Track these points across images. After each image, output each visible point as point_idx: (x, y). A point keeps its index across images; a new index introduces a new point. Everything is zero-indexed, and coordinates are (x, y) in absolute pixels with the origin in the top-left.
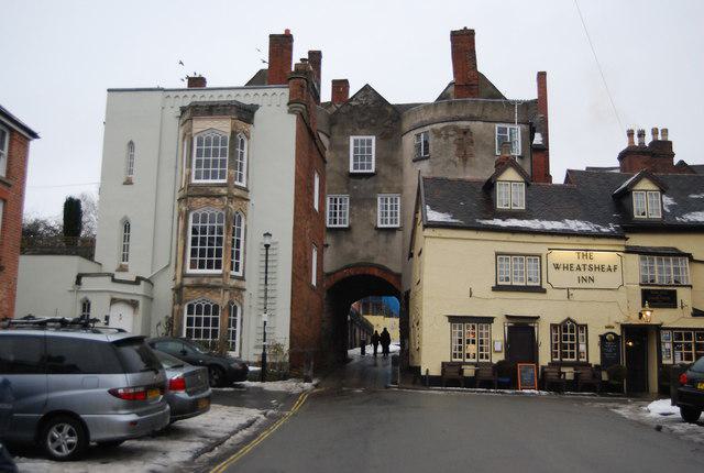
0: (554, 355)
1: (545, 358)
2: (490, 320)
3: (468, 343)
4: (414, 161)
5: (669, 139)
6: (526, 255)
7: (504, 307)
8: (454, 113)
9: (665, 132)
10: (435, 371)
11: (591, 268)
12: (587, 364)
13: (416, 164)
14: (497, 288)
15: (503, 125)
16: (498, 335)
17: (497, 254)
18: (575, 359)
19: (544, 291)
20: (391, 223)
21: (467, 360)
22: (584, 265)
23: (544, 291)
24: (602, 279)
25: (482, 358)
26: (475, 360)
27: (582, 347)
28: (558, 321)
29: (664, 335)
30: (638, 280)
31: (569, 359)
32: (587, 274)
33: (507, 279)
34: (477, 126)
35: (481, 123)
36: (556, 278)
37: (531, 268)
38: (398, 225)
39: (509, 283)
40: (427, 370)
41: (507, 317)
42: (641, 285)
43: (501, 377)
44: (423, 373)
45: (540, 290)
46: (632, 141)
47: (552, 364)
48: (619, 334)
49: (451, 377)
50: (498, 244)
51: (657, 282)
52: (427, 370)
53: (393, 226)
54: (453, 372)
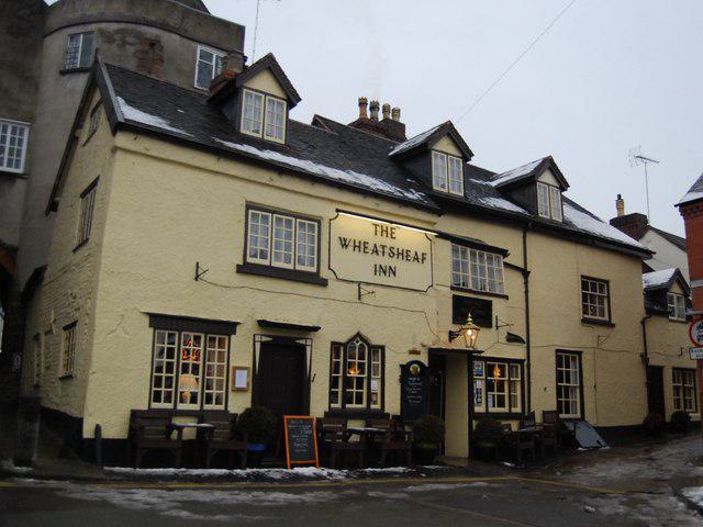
0: (333, 397)
1: (319, 404)
2: (229, 328)
3: (185, 370)
4: (63, 73)
5: (401, 121)
6: (297, 216)
7: (257, 305)
8: (139, 12)
9: (397, 112)
10: (116, 428)
11: (392, 254)
12: (381, 415)
13: (65, 78)
14: (245, 269)
15: (208, 49)
16: (243, 353)
17: (249, 206)
18: (364, 405)
19: (324, 283)
20: (9, 165)
21: (181, 407)
22: (383, 247)
23: (324, 283)
24: (408, 273)
25: (209, 399)
26: (196, 407)
27: (375, 385)
28: (343, 338)
29: (479, 366)
30: (449, 281)
31: (354, 406)
32: (386, 261)
33: (263, 256)
34: (171, 41)
35: (178, 37)
36: (345, 264)
37: (301, 240)
38: (20, 171)
39: (266, 262)
40: (98, 429)
41: (263, 324)
42: (452, 288)
43: (253, 441)
44: (88, 432)
45: (315, 280)
46: (363, 113)
47: (331, 414)
48: (426, 364)
49: (149, 443)
50: (252, 187)
51: (470, 287)
52: (98, 429)
53: (12, 170)
54: (152, 432)
